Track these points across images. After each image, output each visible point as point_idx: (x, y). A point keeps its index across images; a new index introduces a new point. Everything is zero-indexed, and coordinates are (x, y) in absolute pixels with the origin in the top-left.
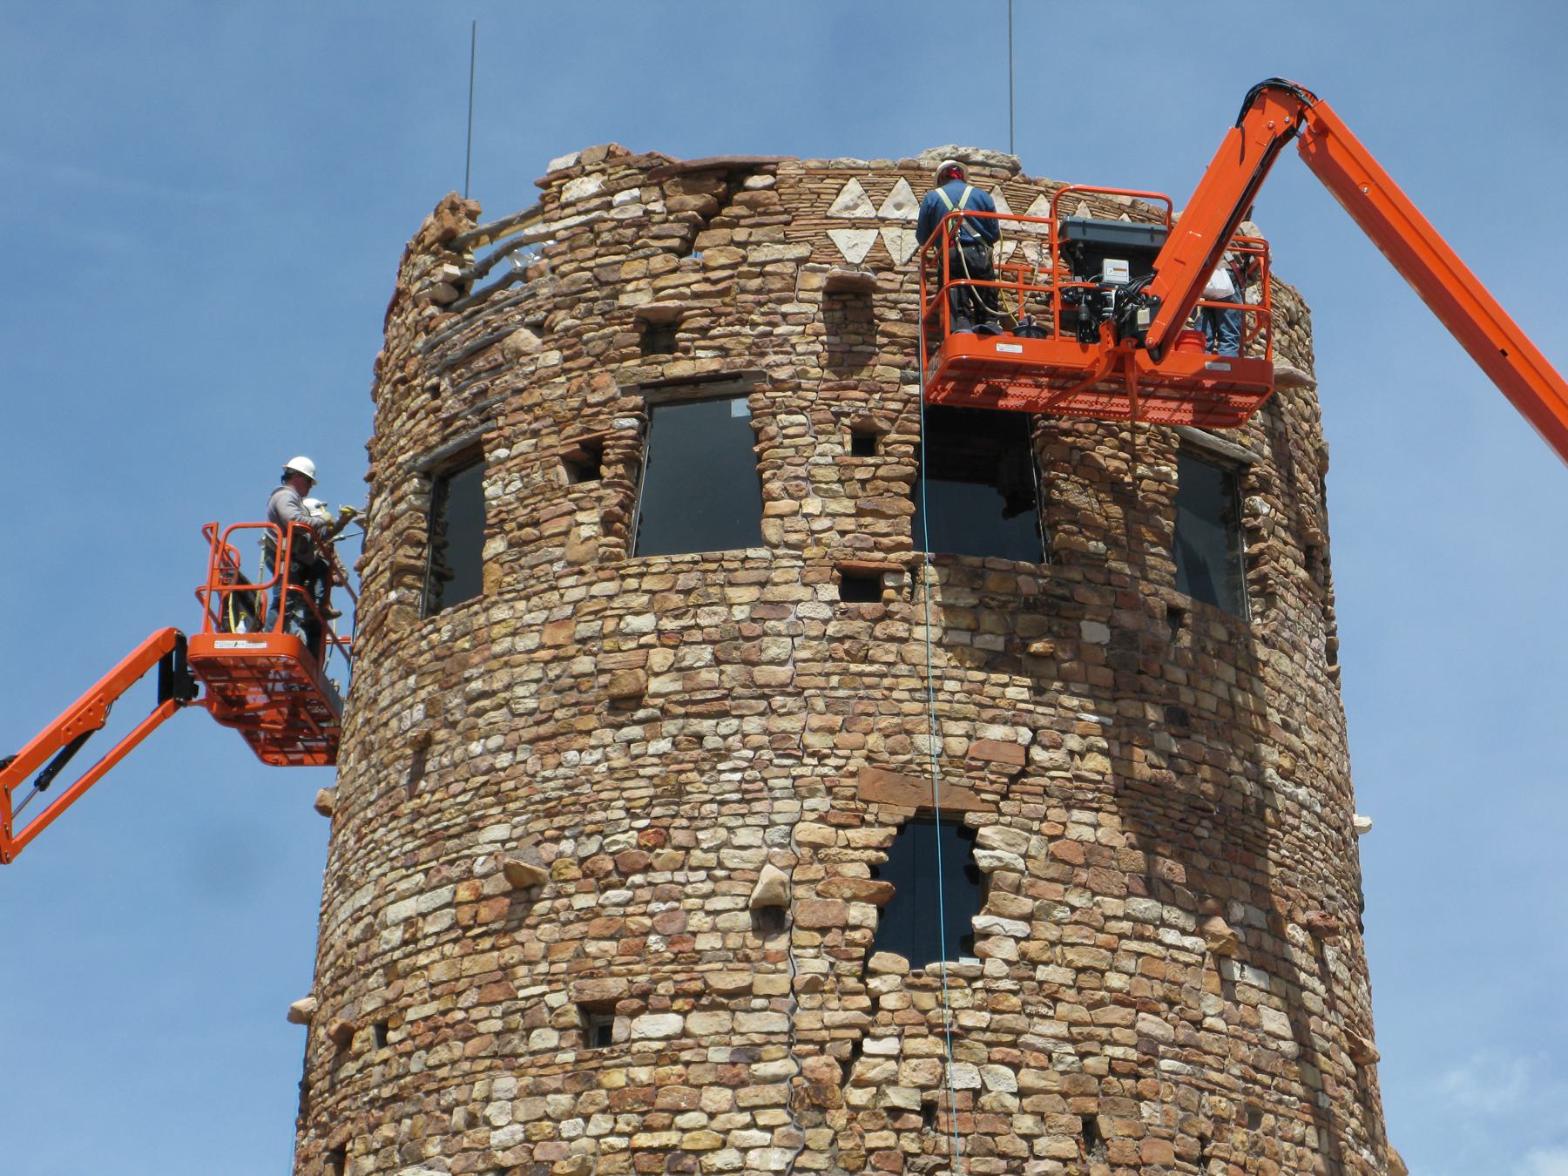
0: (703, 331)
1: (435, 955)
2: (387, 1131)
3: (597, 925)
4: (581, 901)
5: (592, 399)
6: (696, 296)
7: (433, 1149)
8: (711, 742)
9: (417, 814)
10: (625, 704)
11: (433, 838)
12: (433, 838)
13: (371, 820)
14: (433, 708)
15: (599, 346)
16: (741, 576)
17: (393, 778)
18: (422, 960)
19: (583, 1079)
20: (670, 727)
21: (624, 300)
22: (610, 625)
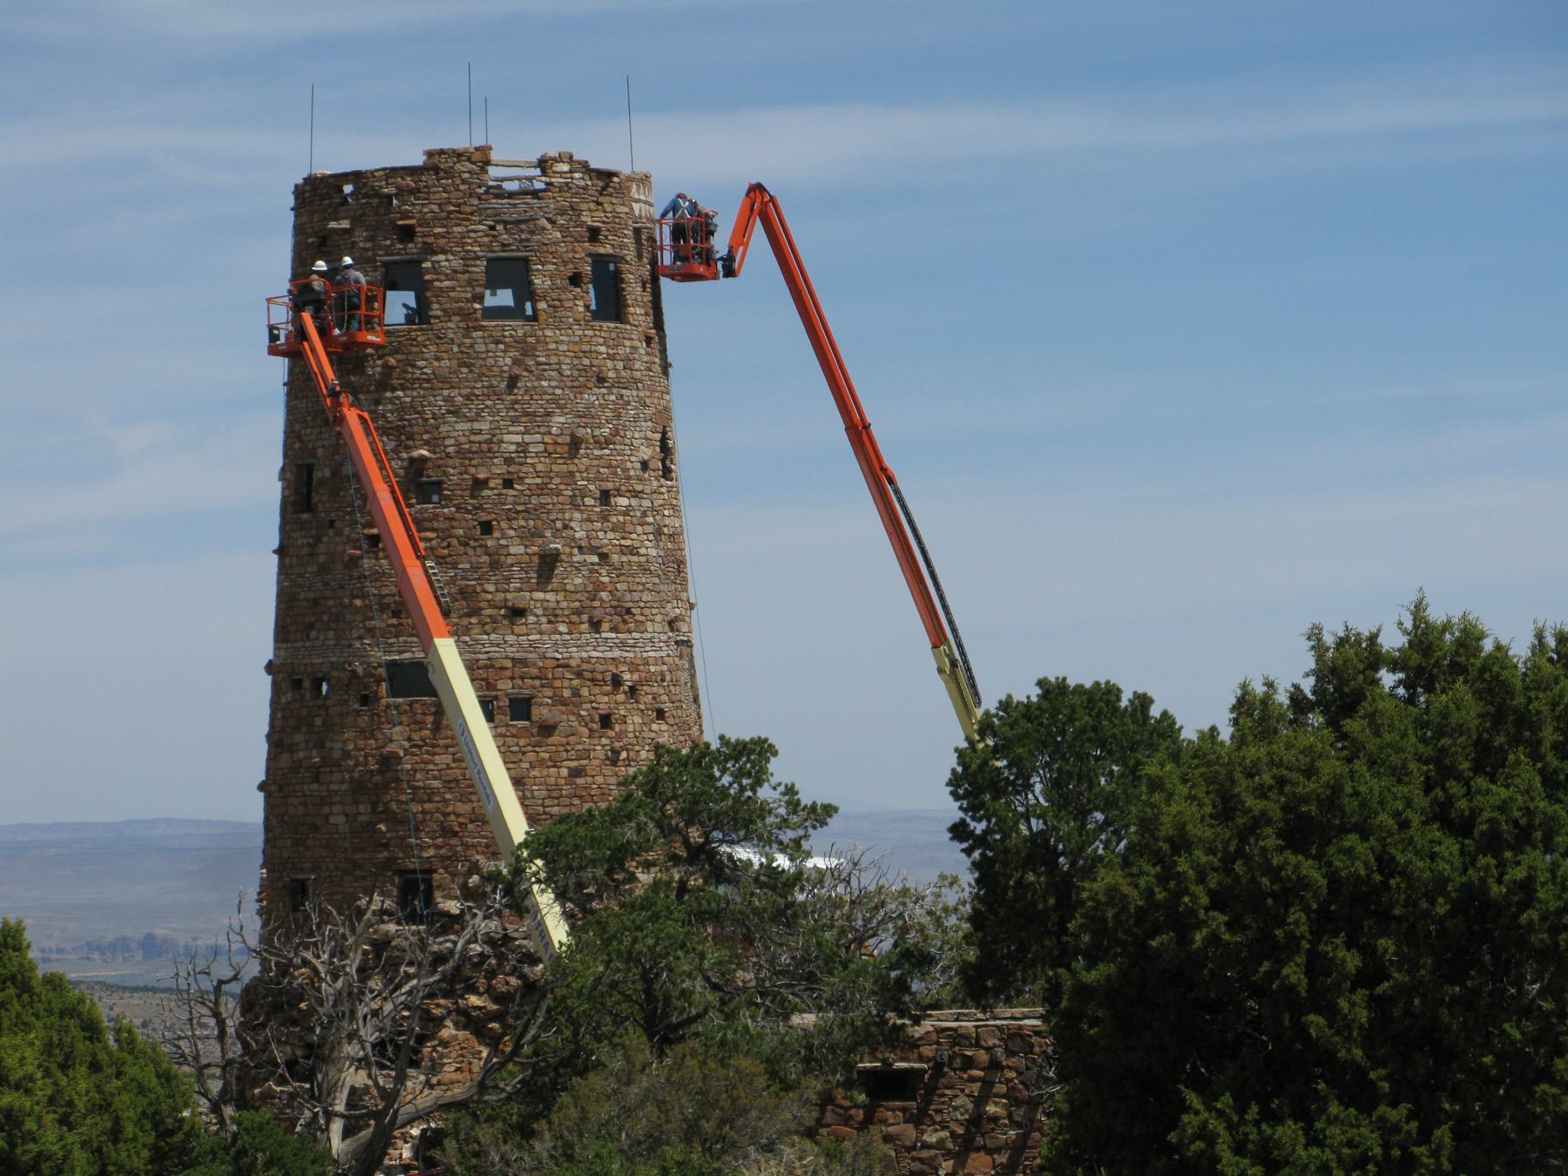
0: (606, 237)
1: (536, 460)
2: (522, 523)
3: (602, 462)
4: (597, 452)
5: (577, 256)
6: (603, 222)
7: (548, 534)
8: (625, 398)
9: (516, 402)
10: (601, 380)
11: (527, 414)
12: (527, 414)
13: (477, 396)
14: (516, 362)
15: (576, 235)
16: (626, 336)
17: (495, 383)
18: (529, 461)
19: (604, 518)
20: (615, 390)
21: (583, 219)
22: (594, 348)
